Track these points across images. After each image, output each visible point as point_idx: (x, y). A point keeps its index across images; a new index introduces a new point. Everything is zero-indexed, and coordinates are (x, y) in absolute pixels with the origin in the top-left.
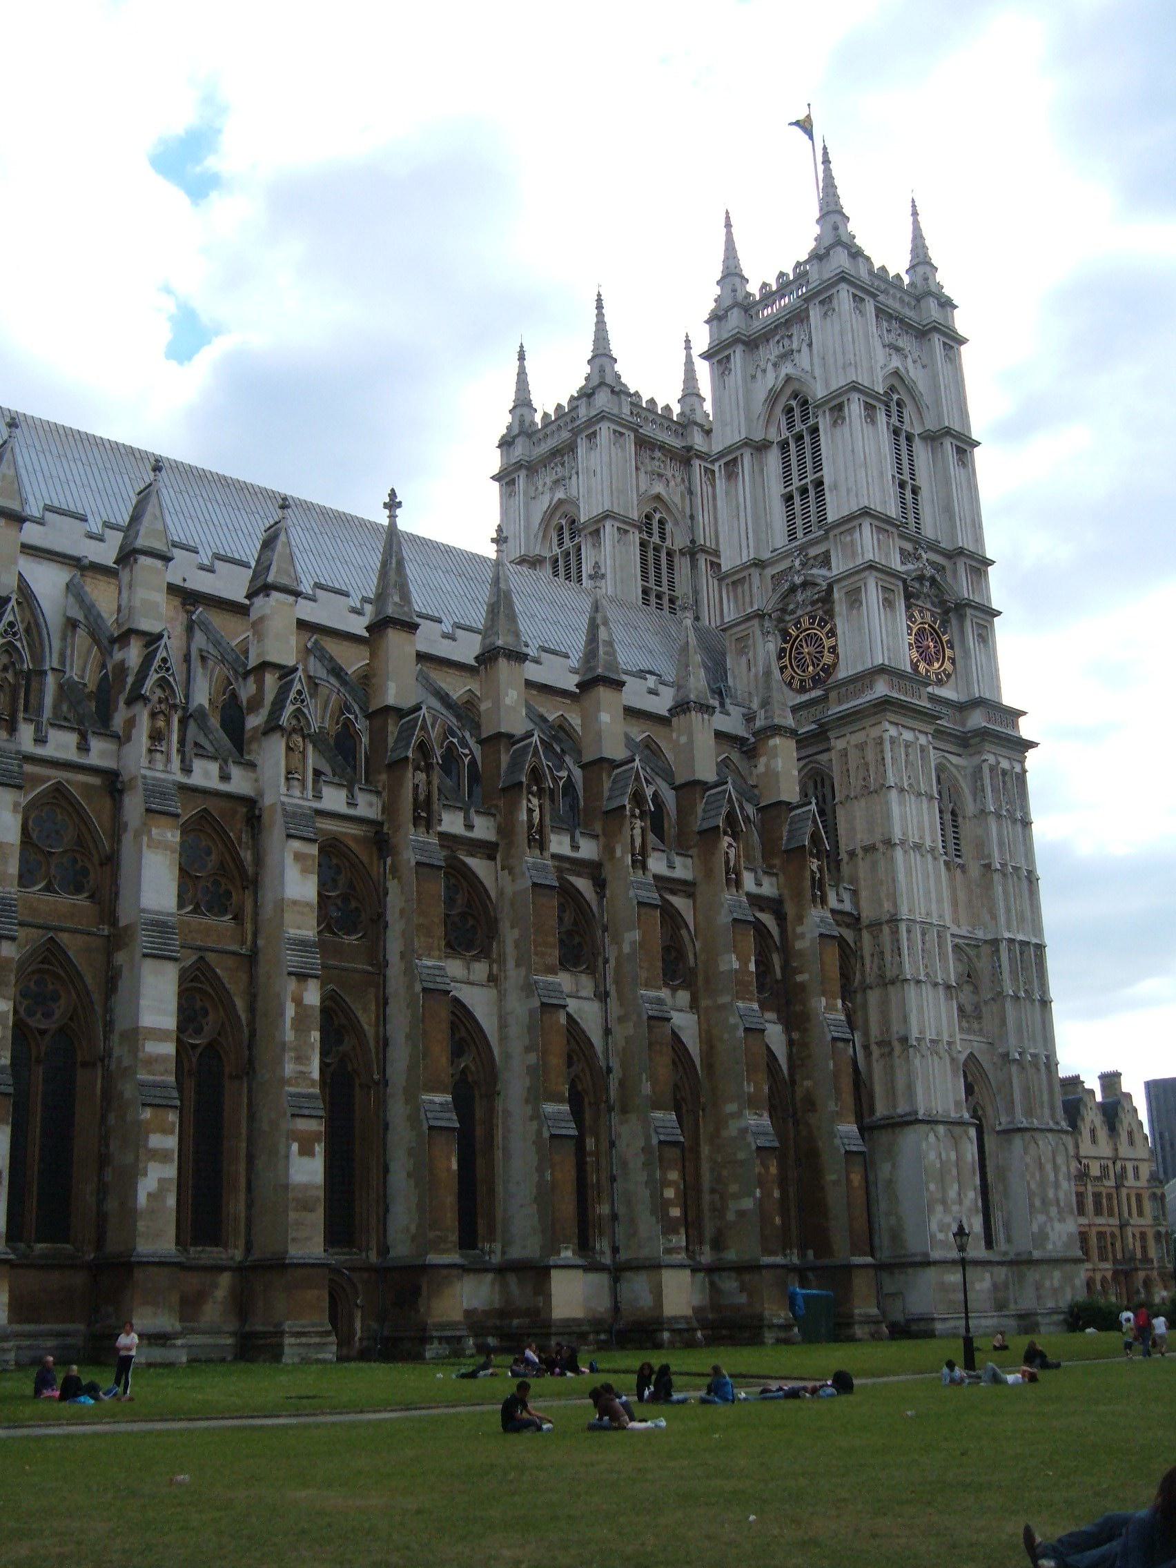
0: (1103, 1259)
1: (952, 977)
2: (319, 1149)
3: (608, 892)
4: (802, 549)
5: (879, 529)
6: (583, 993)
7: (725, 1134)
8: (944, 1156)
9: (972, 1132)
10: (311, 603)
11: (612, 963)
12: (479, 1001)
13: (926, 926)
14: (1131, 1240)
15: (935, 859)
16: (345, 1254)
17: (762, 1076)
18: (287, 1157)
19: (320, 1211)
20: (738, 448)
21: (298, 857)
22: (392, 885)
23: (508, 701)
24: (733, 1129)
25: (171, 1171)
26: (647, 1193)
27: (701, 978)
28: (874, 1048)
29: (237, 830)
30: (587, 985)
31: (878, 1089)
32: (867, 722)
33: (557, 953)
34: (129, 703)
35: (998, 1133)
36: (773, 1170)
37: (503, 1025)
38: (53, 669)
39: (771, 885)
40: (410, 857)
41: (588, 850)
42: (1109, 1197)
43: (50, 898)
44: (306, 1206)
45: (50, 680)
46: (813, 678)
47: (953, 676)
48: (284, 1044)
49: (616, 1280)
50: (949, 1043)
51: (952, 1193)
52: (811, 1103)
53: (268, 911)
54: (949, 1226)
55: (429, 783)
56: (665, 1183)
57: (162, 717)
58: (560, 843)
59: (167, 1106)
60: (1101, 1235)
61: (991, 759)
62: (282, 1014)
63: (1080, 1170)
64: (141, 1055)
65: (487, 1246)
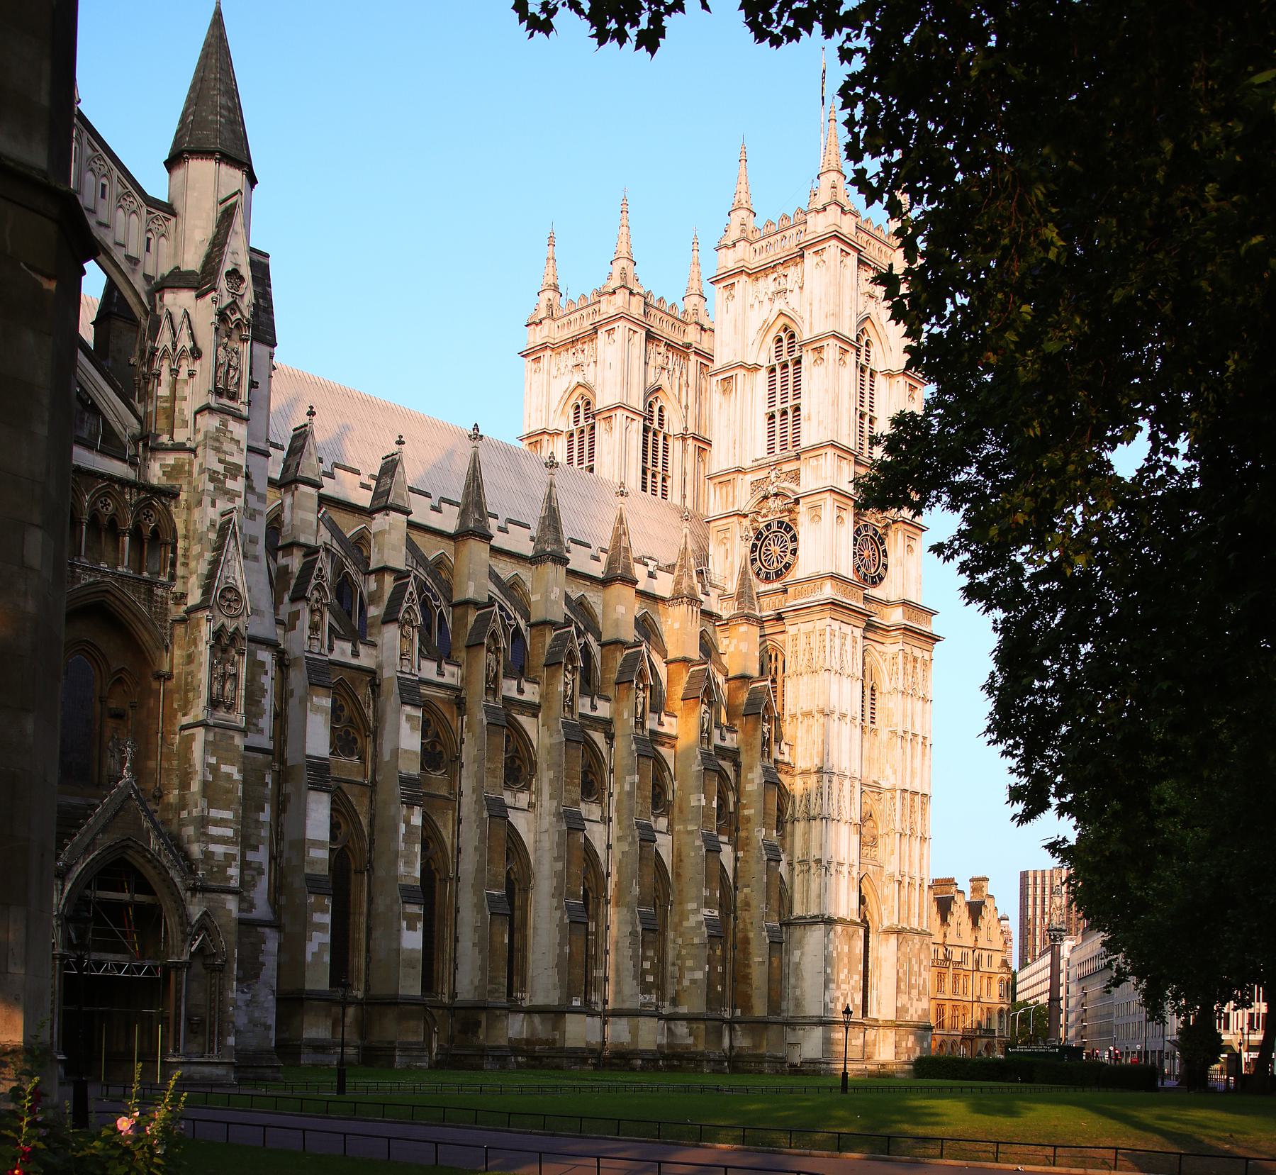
2: (420, 925)
3: (615, 744)
7: (685, 924)
11: (615, 796)
12: (520, 821)
17: (716, 884)
18: (399, 931)
21: (409, 718)
23: (553, 597)
24: (692, 921)
25: (326, 938)
27: (676, 810)
29: (363, 693)
32: (816, 617)
36: (718, 952)
39: (732, 740)
41: (603, 710)
44: (410, 964)
49: (605, 1023)
53: (386, 756)
55: (498, 663)
56: (644, 958)
62: (396, 831)
65: (519, 995)
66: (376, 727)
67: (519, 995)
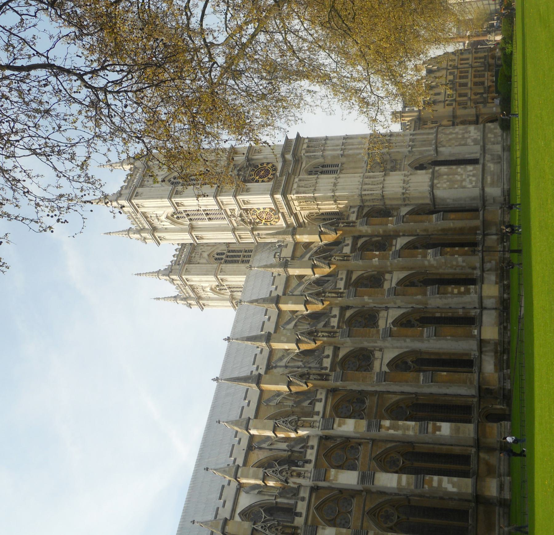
0: (483, 76)
1: (381, 173)
2: (438, 424)
3: (351, 305)
4: (228, 216)
5: (221, 192)
6: (386, 315)
7: (435, 265)
8: (445, 181)
9: (437, 168)
10: (251, 402)
12: (389, 356)
13: (363, 183)
14: (477, 64)
15: (339, 177)
16: (474, 410)
18: (441, 436)
19: (459, 424)
20: (192, 235)
21: (339, 425)
22: (348, 388)
25: (445, 479)
26: (455, 298)
28: (406, 202)
29: (331, 444)
30: (383, 314)
31: (421, 202)
33: (372, 329)
34: (287, 483)
35: (437, 155)
36: (448, 249)
37: (397, 348)
38: (275, 499)
39: (348, 240)
40: (339, 383)
42: (461, 72)
43: (354, 512)
44: (458, 430)
45: (279, 500)
46: (274, 215)
47: (274, 164)
48: (403, 434)
49: (485, 308)
50: (405, 176)
51: (459, 178)
52: (425, 230)
53: (358, 435)
54: (470, 180)
55: (314, 374)
56: (452, 293)
57: (293, 473)
58: (334, 322)
59: (423, 480)
60: (475, 76)
61: (303, 152)
62: (393, 434)
63: (451, 84)
64: (406, 487)
66: (345, 437)
67: (472, 356)
